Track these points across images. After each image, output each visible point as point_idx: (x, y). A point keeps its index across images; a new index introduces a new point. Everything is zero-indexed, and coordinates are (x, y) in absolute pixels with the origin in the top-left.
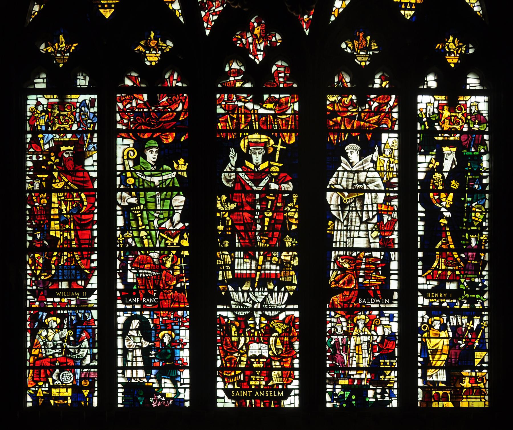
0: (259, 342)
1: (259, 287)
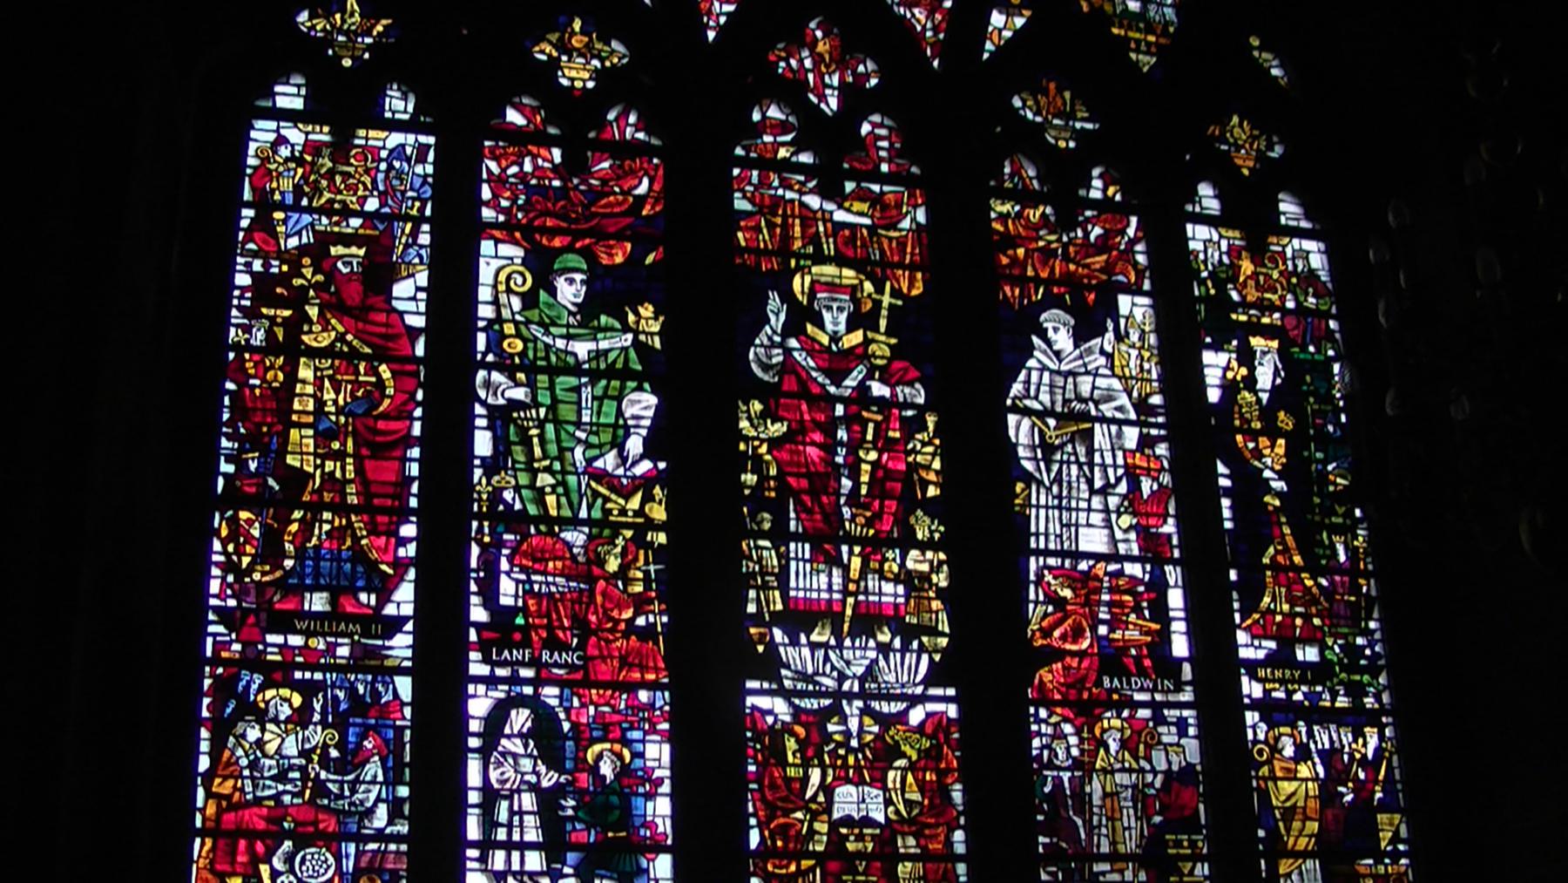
0: (859, 782)
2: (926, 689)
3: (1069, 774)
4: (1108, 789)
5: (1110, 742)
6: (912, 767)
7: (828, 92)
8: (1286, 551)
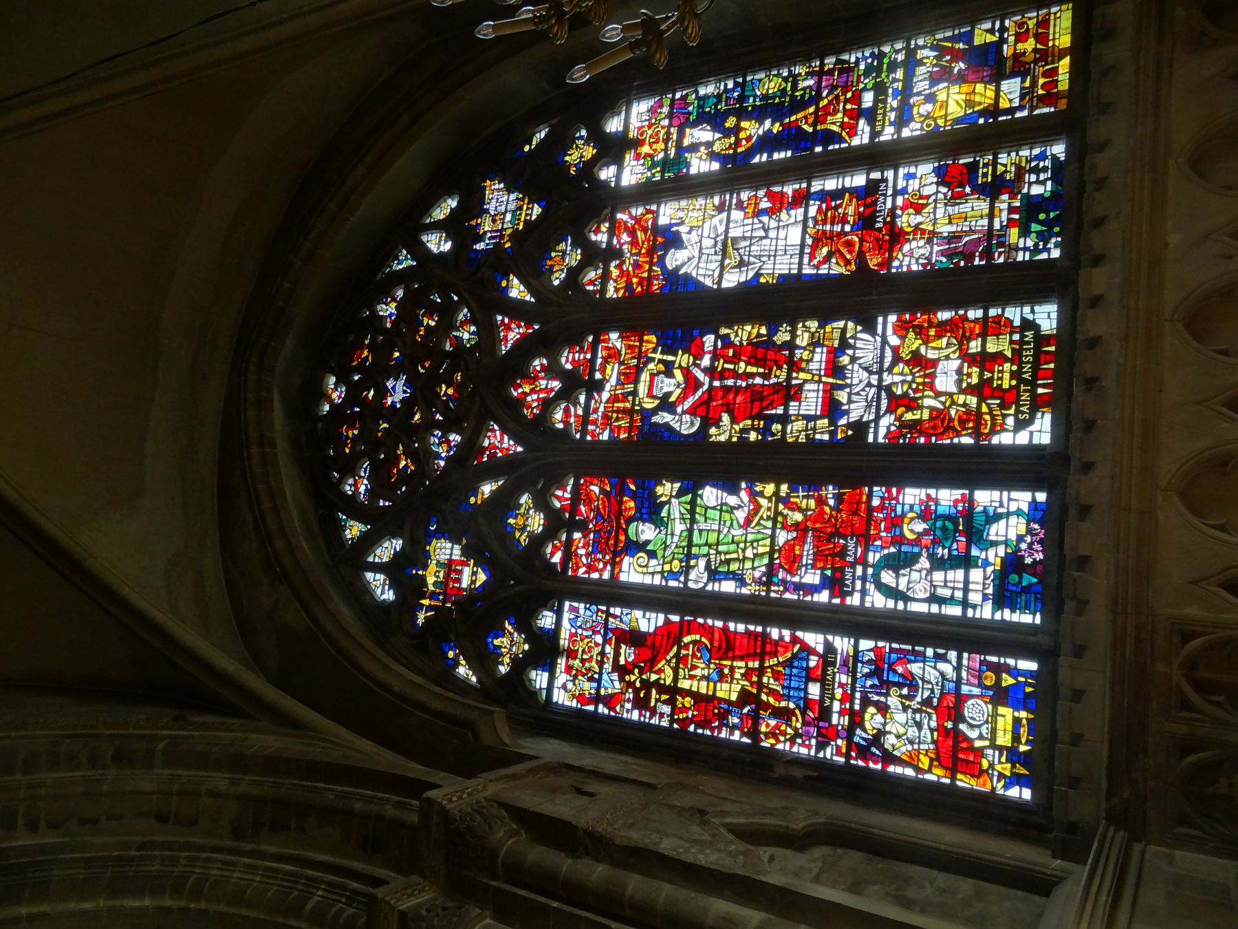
0: (932, 376)
1: (844, 378)
2: (878, 335)
3: (935, 246)
4: (947, 221)
5: (916, 222)
6: (926, 341)
7: (549, 387)
8: (806, 117)
